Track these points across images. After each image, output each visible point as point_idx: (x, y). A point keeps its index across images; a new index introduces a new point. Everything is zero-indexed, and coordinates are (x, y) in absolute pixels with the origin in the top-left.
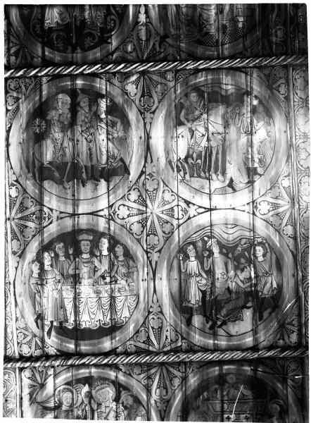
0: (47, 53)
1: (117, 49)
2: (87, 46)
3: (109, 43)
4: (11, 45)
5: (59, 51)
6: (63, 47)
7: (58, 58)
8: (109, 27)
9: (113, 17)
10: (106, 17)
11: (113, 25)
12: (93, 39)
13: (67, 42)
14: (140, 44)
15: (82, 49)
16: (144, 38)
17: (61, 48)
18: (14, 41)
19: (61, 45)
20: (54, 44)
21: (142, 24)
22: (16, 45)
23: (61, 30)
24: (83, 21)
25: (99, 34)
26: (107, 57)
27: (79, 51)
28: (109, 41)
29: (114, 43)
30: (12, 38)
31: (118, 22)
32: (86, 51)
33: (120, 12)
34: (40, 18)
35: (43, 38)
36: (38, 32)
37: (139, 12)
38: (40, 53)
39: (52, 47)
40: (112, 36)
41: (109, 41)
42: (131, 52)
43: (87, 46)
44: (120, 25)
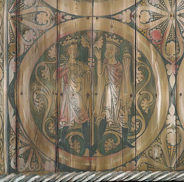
0: (60, 156)
1: (142, 154)
2: (107, 149)
3: (132, 147)
4: (20, 145)
5: (74, 153)
6: (80, 149)
7: (72, 165)
8: (133, 129)
9: (138, 117)
10: (130, 116)
11: (138, 126)
12: (115, 142)
13: (85, 144)
14: (169, 150)
15: (101, 152)
16: (173, 143)
17: (78, 151)
18: (24, 141)
19: (77, 147)
20: (69, 145)
21: (171, 127)
22: (26, 145)
23: (77, 130)
24: (104, 122)
25: (121, 136)
26: (130, 162)
27: (98, 154)
28: (133, 144)
29: (140, 147)
30: (20, 138)
31: (143, 122)
32: (107, 155)
33: (147, 112)
34: (54, 115)
35: (57, 139)
36: (52, 132)
37: (169, 113)
38: (53, 156)
39: (67, 149)
40: (136, 139)
41: (133, 144)
42: (157, 158)
43: (107, 149)
44: (147, 124)
